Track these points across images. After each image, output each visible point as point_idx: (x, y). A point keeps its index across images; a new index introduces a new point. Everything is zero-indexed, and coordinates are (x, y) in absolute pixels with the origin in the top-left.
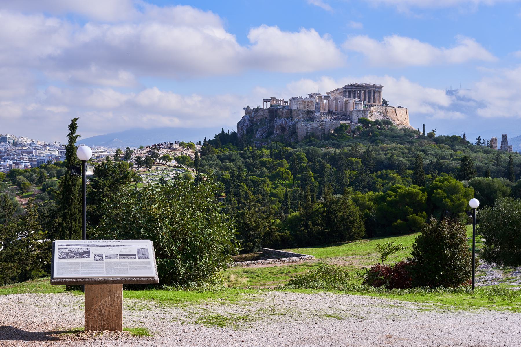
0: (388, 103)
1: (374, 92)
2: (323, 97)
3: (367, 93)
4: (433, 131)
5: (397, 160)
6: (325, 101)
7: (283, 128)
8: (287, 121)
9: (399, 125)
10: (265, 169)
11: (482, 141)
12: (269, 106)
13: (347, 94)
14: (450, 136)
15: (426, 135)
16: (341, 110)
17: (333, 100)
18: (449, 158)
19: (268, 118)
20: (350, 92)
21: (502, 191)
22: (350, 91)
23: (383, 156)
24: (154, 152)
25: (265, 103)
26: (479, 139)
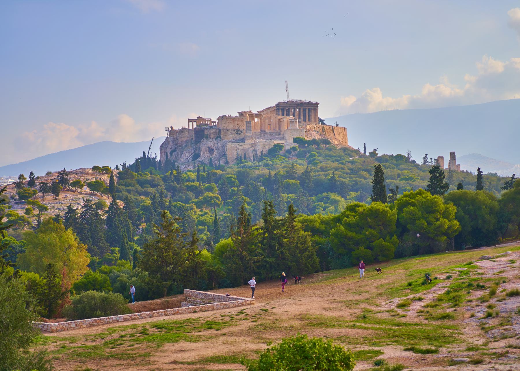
0: (325, 122)
1: (309, 110)
2: (254, 115)
3: (302, 110)
5: (339, 181)
6: (256, 120)
8: (216, 142)
10: (191, 194)
11: (429, 160)
12: (195, 126)
13: (281, 113)
15: (367, 154)
17: (265, 119)
18: (396, 177)
20: (283, 110)
22: (283, 108)
23: (323, 177)
24: (63, 178)
25: (191, 123)
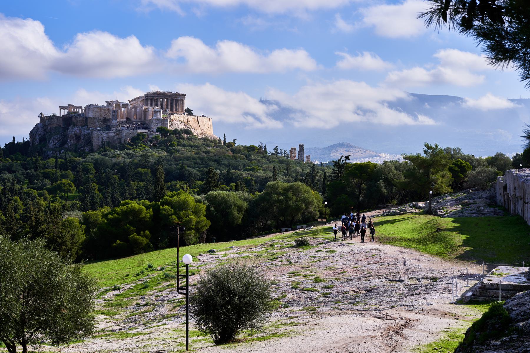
0: (192, 112)
1: (177, 101)
3: (169, 101)
4: (234, 140)
5: (187, 170)
6: (123, 109)
7: (78, 137)
8: (82, 130)
9: (201, 134)
10: (47, 181)
11: (279, 151)
12: (66, 113)
13: (149, 102)
14: (248, 145)
16: (140, 119)
17: (132, 108)
18: (242, 168)
19: (62, 126)
20: (152, 100)
21: (238, 206)
22: (152, 98)
23: (174, 167)
25: (62, 111)
26: (276, 149)
